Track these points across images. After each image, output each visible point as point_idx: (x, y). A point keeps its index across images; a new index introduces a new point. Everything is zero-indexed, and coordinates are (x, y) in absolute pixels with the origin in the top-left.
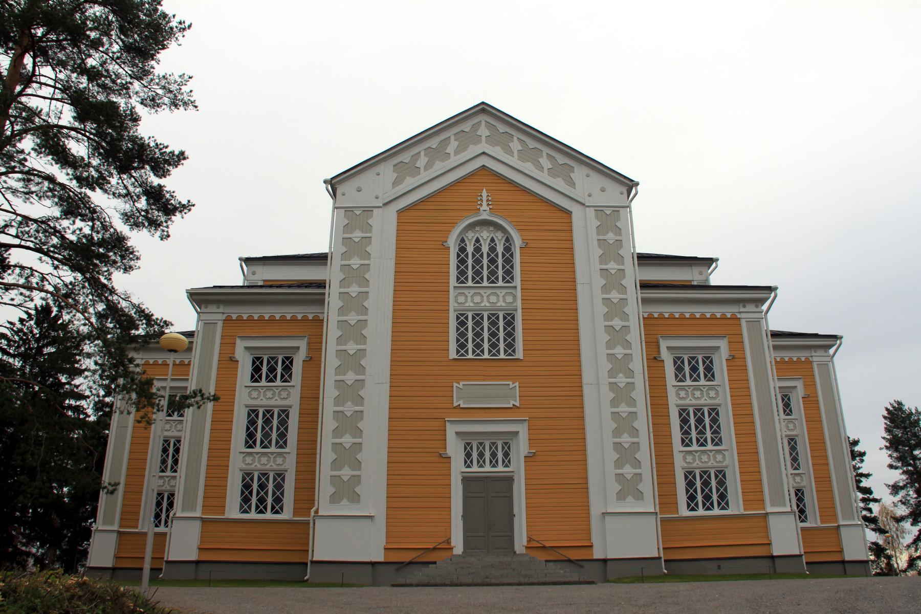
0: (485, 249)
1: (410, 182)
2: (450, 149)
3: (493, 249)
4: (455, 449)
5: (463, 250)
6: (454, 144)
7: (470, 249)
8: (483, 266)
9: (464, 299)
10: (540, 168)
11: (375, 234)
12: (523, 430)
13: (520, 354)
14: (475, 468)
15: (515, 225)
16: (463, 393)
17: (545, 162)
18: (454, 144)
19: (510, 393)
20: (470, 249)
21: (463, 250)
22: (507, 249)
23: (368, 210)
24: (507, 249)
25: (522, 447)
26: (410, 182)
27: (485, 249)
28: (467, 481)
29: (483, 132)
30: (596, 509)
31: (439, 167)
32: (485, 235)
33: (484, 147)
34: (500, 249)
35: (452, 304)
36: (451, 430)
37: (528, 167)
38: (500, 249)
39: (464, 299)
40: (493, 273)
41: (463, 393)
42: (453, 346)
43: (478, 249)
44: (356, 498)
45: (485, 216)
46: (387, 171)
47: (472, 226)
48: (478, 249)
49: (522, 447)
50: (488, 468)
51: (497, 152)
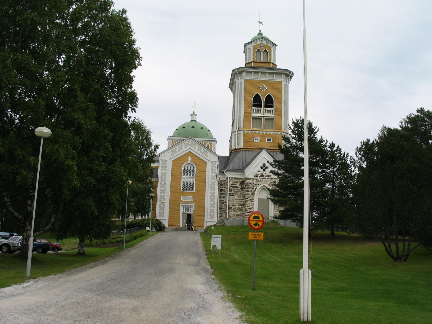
0: (189, 169)
1: (175, 154)
2: (183, 147)
3: (190, 169)
4: (181, 208)
5: (185, 169)
6: (184, 146)
7: (186, 169)
8: (189, 172)
9: (185, 179)
10: (201, 152)
11: (167, 166)
12: (194, 205)
13: (194, 191)
14: (185, 212)
15: (196, 164)
16: (183, 198)
17: (202, 151)
18: (184, 146)
19: (191, 198)
20: (186, 169)
21: (185, 169)
22: (193, 169)
23: (166, 161)
24: (193, 169)
25: (193, 209)
26: (175, 154)
27: (189, 169)
28: (183, 214)
29: (190, 143)
30: (205, 221)
31: (181, 151)
32: (189, 166)
33: (190, 147)
34: (192, 169)
35: (182, 180)
36: (180, 205)
37: (199, 152)
38: (192, 169)
39: (185, 179)
40: (190, 174)
41: (183, 198)
42: (182, 189)
43: (188, 169)
44: (163, 216)
45: (189, 162)
46: (170, 151)
47: (187, 164)
48: (188, 169)
49: (193, 209)
50: (187, 212)
51: (193, 148)
